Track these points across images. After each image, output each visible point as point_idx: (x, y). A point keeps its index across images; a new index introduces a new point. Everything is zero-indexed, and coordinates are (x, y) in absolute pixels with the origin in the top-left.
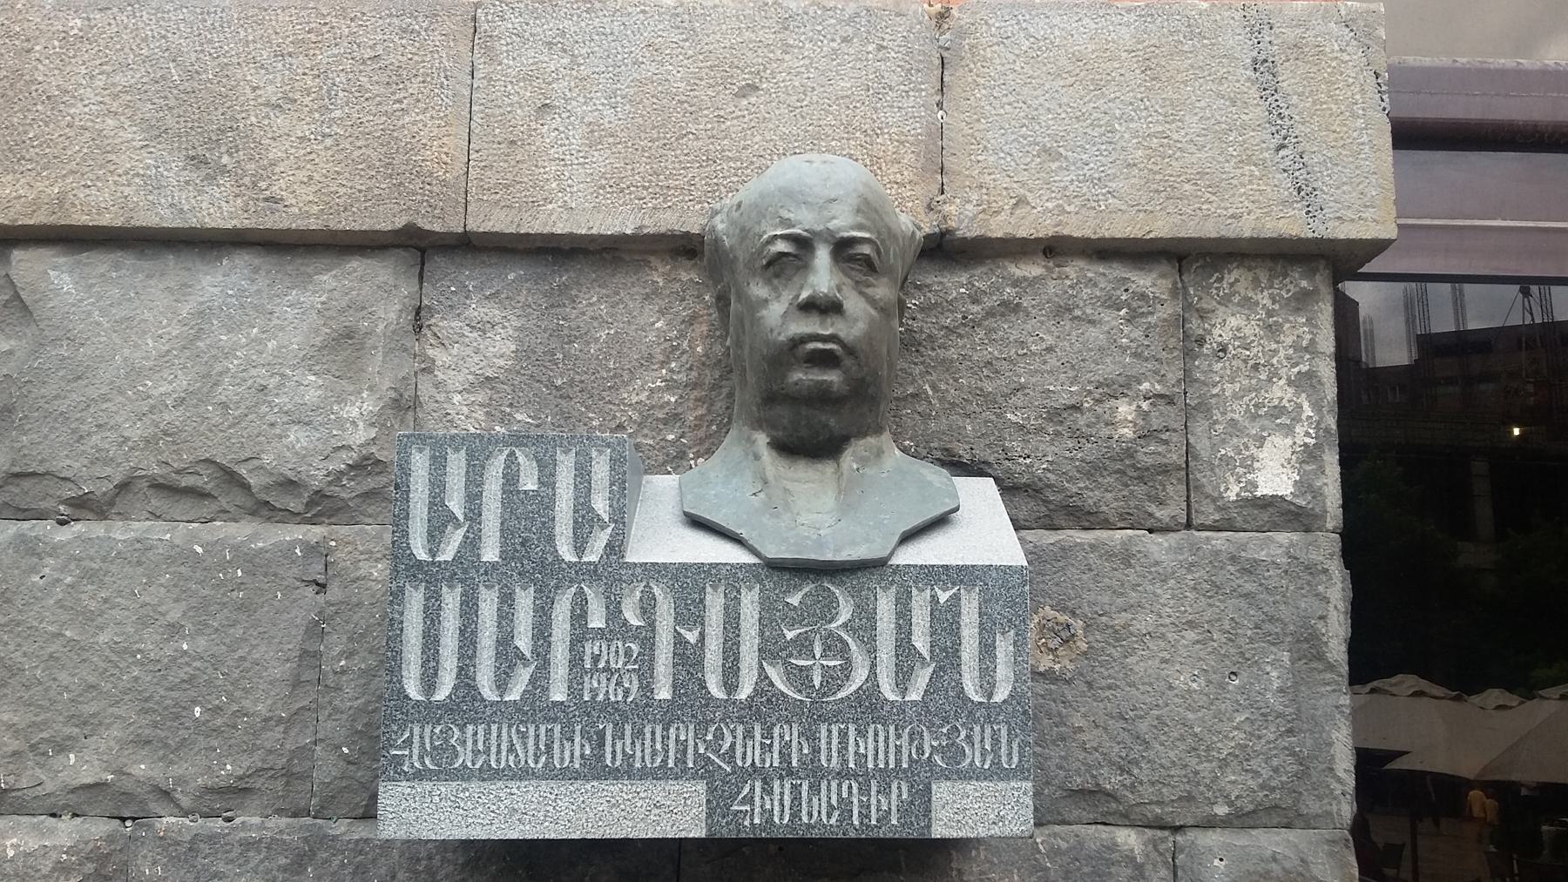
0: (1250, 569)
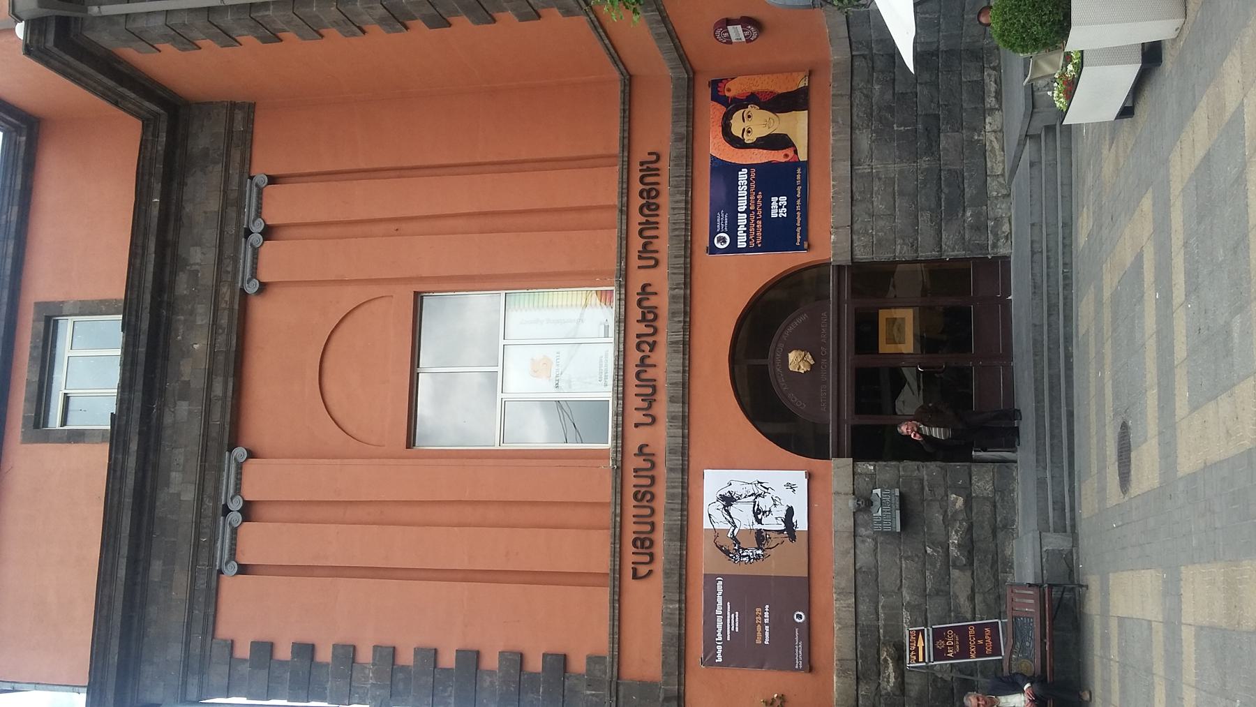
0: (879, 470)
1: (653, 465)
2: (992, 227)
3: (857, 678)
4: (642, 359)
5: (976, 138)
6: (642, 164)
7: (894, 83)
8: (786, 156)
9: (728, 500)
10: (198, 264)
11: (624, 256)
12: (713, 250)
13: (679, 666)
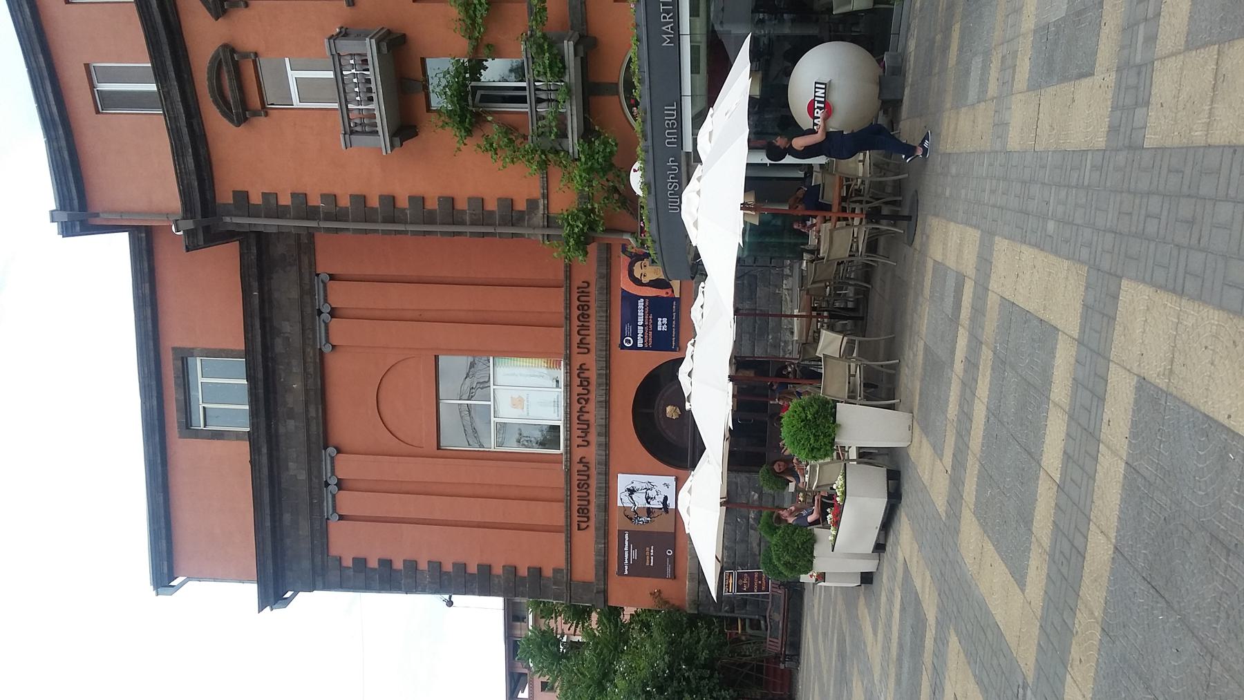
1: (588, 468)
3: (699, 582)
4: (581, 408)
5: (777, 292)
6: (578, 288)
8: (667, 293)
9: (631, 491)
10: (289, 333)
11: (568, 346)
12: (623, 347)
13: (604, 575)
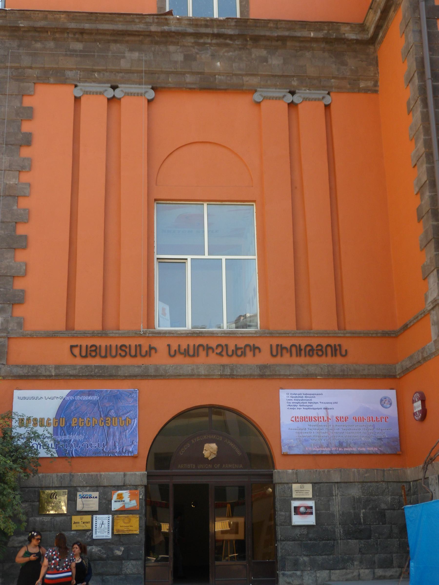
2: (296, 574)
6: (340, 345)
7: (391, 509)
